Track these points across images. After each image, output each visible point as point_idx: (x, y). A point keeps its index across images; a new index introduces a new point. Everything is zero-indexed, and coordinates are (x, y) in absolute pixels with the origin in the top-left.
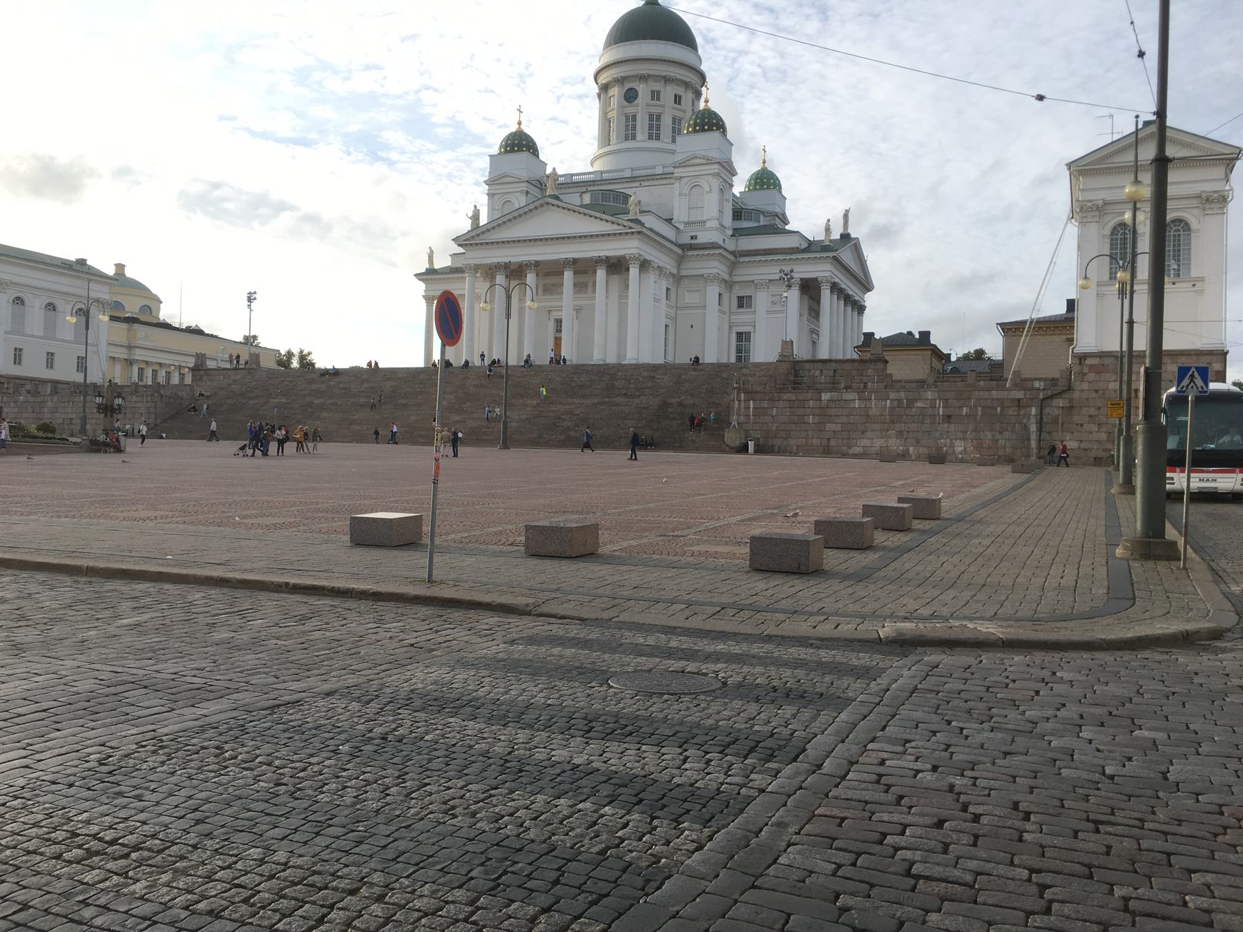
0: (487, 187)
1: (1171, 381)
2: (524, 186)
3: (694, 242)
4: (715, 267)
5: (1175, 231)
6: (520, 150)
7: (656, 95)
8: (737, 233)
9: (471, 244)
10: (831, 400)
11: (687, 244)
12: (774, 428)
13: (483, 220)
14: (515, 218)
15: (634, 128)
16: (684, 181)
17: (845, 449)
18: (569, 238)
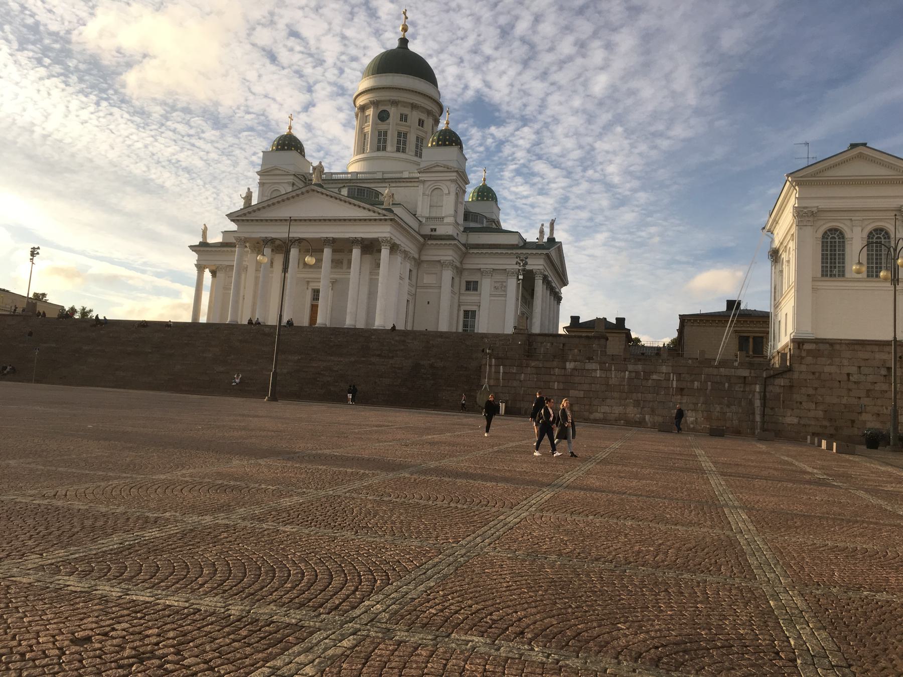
0: (259, 177)
1: (879, 368)
2: (291, 179)
3: (433, 233)
4: (448, 255)
6: (289, 149)
8: (467, 230)
9: (243, 220)
10: (575, 369)
12: (522, 392)
13: (254, 201)
14: (283, 201)
15: (385, 141)
16: (427, 184)
17: (586, 414)
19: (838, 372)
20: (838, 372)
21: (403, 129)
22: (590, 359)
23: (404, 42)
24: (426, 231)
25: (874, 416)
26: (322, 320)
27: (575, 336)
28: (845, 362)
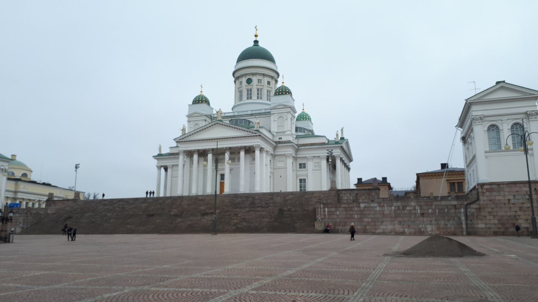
0: (187, 118)
1: (524, 195)
3: (280, 140)
7: (260, 81)
8: (297, 137)
9: (182, 142)
10: (365, 207)
12: (338, 221)
14: (203, 130)
15: (251, 94)
16: (275, 115)
17: (374, 230)
18: (227, 138)
20: (503, 199)
22: (373, 201)
23: (256, 42)
24: (277, 139)
25: (525, 221)
26: (227, 190)
27: (362, 190)
28: (507, 194)
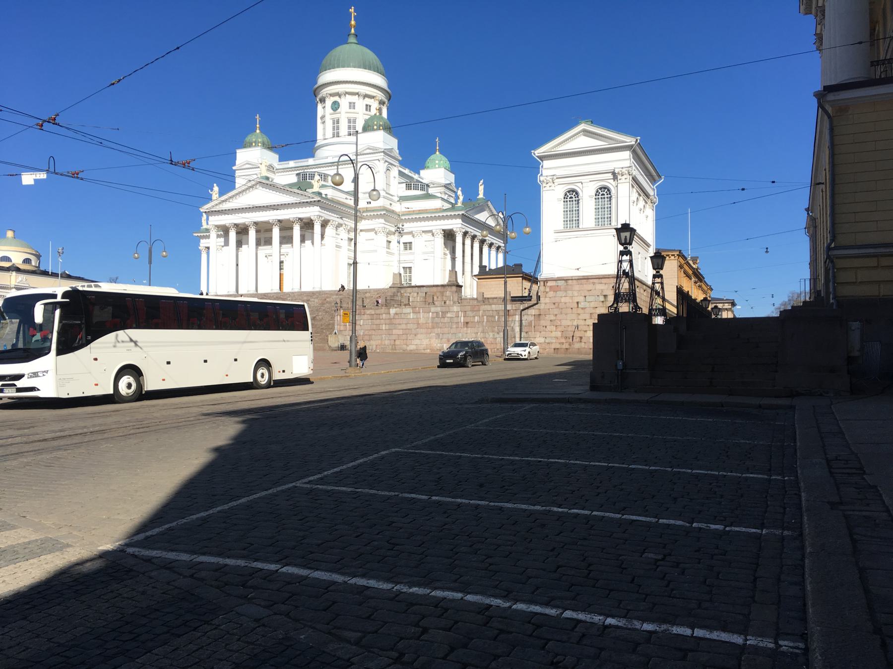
1: (598, 296)
3: (369, 206)
5: (602, 195)
7: (352, 105)
11: (365, 208)
12: (362, 334)
19: (571, 301)
20: (571, 301)
21: (352, 116)
28: (576, 294)
